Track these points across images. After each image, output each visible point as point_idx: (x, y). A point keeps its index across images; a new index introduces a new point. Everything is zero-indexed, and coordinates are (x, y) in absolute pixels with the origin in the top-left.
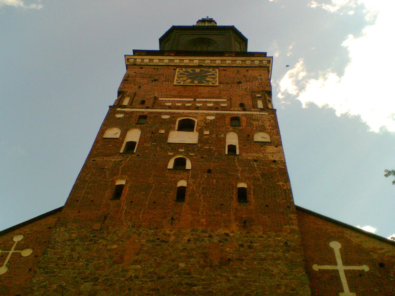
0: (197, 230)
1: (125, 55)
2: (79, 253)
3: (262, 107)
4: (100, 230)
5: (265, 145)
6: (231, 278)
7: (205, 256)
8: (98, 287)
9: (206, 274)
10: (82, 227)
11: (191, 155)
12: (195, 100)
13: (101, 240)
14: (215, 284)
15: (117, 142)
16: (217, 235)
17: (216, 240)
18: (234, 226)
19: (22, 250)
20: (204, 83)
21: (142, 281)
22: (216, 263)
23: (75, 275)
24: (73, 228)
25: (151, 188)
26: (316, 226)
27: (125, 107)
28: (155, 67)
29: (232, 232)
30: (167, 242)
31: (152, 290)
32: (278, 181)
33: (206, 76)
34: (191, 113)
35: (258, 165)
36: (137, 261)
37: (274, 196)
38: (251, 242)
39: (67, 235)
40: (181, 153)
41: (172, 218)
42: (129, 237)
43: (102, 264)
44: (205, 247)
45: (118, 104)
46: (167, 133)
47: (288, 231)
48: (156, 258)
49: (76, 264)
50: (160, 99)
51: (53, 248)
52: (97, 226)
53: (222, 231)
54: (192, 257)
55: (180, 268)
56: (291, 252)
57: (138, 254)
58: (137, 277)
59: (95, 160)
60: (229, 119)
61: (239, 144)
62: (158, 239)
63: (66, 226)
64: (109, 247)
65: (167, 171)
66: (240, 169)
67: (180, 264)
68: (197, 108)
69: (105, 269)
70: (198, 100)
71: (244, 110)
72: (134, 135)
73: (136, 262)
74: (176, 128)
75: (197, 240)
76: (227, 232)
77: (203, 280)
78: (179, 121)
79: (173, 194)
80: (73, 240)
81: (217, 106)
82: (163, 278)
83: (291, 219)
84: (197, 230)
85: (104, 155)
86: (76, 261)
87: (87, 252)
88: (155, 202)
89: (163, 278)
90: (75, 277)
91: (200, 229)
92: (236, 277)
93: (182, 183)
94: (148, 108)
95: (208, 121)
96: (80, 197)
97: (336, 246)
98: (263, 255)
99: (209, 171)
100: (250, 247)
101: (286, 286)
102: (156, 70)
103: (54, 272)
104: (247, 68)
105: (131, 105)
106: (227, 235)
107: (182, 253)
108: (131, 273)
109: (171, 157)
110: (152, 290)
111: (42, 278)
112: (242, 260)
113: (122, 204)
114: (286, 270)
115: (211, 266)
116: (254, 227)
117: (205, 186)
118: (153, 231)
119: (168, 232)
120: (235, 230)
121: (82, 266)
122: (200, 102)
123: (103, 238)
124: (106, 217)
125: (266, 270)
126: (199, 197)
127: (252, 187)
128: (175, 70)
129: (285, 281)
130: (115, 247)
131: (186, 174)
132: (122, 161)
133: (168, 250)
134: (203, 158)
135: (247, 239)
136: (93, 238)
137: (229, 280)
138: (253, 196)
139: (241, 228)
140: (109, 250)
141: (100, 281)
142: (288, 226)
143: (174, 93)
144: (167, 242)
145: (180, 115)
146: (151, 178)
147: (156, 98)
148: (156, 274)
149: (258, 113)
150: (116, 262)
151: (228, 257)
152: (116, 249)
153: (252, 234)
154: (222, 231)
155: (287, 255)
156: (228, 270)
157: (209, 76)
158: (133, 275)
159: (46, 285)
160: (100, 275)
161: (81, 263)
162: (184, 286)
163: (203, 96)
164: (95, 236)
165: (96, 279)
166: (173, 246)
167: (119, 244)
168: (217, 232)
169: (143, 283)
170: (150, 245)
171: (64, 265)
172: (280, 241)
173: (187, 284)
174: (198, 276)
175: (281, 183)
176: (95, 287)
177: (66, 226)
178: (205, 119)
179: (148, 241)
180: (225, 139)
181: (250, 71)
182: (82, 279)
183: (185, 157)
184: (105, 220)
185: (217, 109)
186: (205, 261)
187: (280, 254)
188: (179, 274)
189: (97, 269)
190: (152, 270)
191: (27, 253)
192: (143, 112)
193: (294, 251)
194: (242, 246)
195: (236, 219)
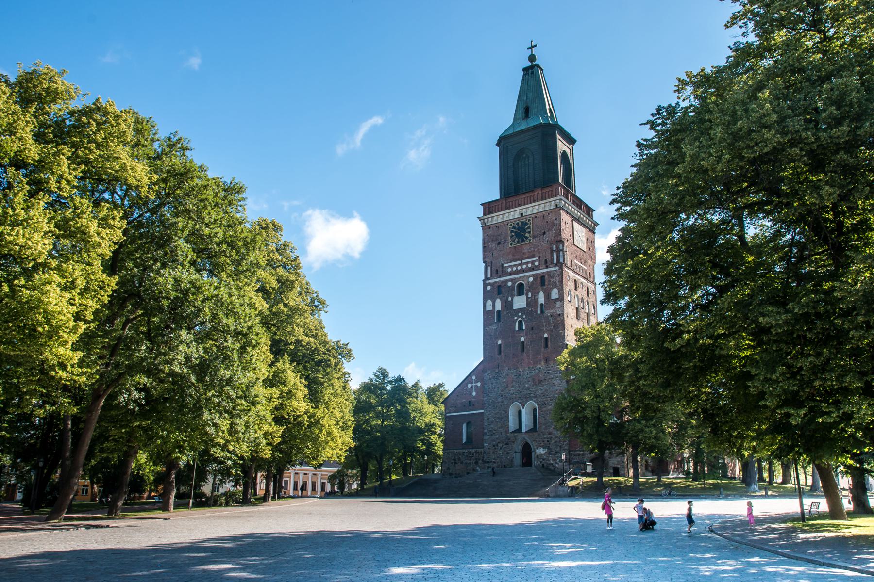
7: (533, 380)
18: (543, 363)
45: (486, 278)
53: (538, 366)
68: (523, 271)
71: (547, 267)
79: (520, 347)
93: (522, 339)
94: (500, 277)
120: (542, 365)
143: (511, 257)
147: (502, 265)
154: (538, 366)
185: (532, 269)
192: (498, 282)
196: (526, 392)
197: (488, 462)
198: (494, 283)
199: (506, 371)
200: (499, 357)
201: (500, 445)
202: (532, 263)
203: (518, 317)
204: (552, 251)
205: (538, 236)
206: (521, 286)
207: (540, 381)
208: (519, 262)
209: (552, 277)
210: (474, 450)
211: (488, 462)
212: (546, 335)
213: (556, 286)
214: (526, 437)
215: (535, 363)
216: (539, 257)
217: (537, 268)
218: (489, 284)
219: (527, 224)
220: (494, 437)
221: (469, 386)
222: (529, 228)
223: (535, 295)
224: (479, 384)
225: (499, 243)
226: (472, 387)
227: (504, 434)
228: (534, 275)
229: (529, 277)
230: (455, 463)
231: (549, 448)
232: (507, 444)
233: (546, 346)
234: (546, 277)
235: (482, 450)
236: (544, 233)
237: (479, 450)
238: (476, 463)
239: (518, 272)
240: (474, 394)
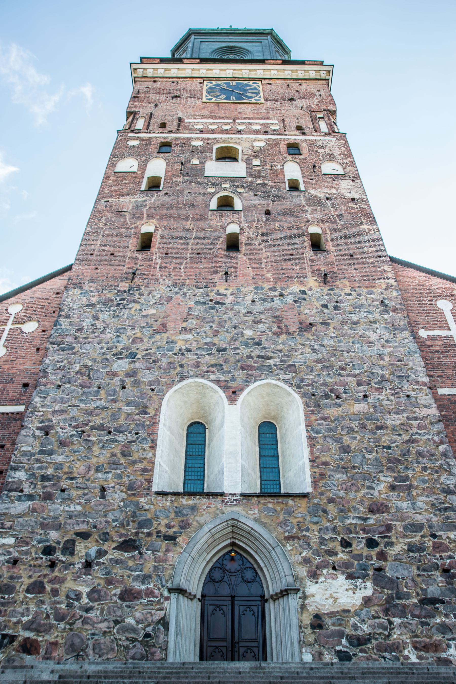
0: (263, 288)
1: (131, 64)
2: (104, 321)
3: (326, 130)
4: (129, 290)
5: (338, 178)
6: (316, 347)
7: (278, 320)
8: (137, 365)
9: (283, 343)
10: (103, 289)
11: (239, 191)
12: (234, 121)
13: (133, 304)
14: (297, 356)
15: (135, 177)
16: (290, 294)
17: (289, 299)
19: (23, 323)
20: (244, 99)
21: (197, 354)
22: (294, 328)
23: (102, 351)
24: (92, 289)
25: (191, 235)
26: (417, 282)
27: (139, 131)
28: (174, 80)
29: (311, 289)
30: (223, 304)
31: (212, 366)
32: (362, 224)
33: (246, 91)
34: (232, 139)
35: (332, 204)
36: (186, 329)
37: (360, 243)
38: (337, 302)
39: (85, 299)
40: (225, 189)
41: (226, 273)
42: (170, 299)
43: (139, 335)
44: (276, 309)
46: (203, 163)
47: (384, 287)
48: (211, 324)
49: (103, 336)
50: (186, 121)
51: (68, 317)
54: (260, 322)
55: (246, 337)
56: (391, 313)
57: (185, 320)
58: (189, 350)
59: (108, 201)
60: (285, 146)
61: (304, 177)
62: (211, 301)
63: (81, 288)
64: (144, 313)
65: (210, 212)
67: (245, 332)
69: (143, 341)
71: (304, 134)
72: (157, 167)
74: (214, 158)
75: (264, 300)
76: (303, 289)
77: (280, 351)
78: (217, 149)
80: (93, 305)
81: (265, 129)
82: (225, 350)
83: (385, 272)
84: (263, 288)
85: (119, 195)
86: (102, 332)
87: (115, 320)
88: (199, 254)
89: (225, 350)
90: (104, 354)
91: (267, 286)
92: (323, 346)
93: (233, 228)
95: (256, 149)
96: (94, 250)
97: (445, 306)
98: (355, 318)
99: (268, 213)
100: (336, 308)
101: (390, 355)
102: (175, 84)
103: (73, 348)
104: (300, 82)
105: (147, 129)
106: (304, 292)
107: (246, 318)
108: (181, 345)
109: (212, 195)
110: (212, 366)
111: (56, 358)
112: (328, 324)
113: (154, 257)
114: (387, 336)
115: (288, 333)
116: (338, 283)
117: (265, 231)
118: (201, 290)
119: (222, 291)
121: (111, 338)
123: (134, 301)
124: (134, 274)
125: (361, 336)
126: (259, 245)
127: (328, 231)
129: (387, 351)
130: (152, 311)
131: (236, 216)
132: (145, 201)
133: (226, 313)
134: (256, 195)
135: (331, 297)
136: (120, 302)
137: (314, 350)
138: (331, 243)
139: (322, 284)
140: (146, 316)
141: (139, 356)
142: (381, 281)
143: (205, 112)
144: (223, 304)
145: (217, 141)
146: (189, 223)
148: (215, 345)
149: (322, 138)
150: (156, 332)
151: (308, 321)
152: (154, 315)
153: (336, 291)
154: (296, 288)
155: (386, 317)
156: (311, 337)
157: (249, 91)
158: (184, 348)
159: (65, 366)
160: (138, 349)
161: (109, 335)
162: (255, 359)
163: (244, 116)
164: (124, 300)
165: (133, 355)
166: (232, 309)
167: (157, 309)
168: (289, 290)
169: (198, 358)
171: (86, 338)
173: (259, 357)
174: (273, 347)
175: (366, 227)
176: (132, 366)
177: (81, 288)
178: (253, 146)
179: (197, 303)
180: (282, 170)
181: (303, 85)
182: (114, 355)
183: (231, 195)
184: (133, 279)
185: (266, 132)
186: (279, 327)
187: (377, 316)
188: (247, 344)
189: (133, 342)
190: (208, 340)
191: (30, 327)
192: (165, 138)
193: (394, 311)
194: (325, 306)
195: (312, 273)
196: (244, 351)
199: (162, 289)
201: (85, 549)
214: (248, 516)
215: (283, 279)
220: (57, 508)
227: (116, 497)
228: (268, 140)
232: (128, 545)
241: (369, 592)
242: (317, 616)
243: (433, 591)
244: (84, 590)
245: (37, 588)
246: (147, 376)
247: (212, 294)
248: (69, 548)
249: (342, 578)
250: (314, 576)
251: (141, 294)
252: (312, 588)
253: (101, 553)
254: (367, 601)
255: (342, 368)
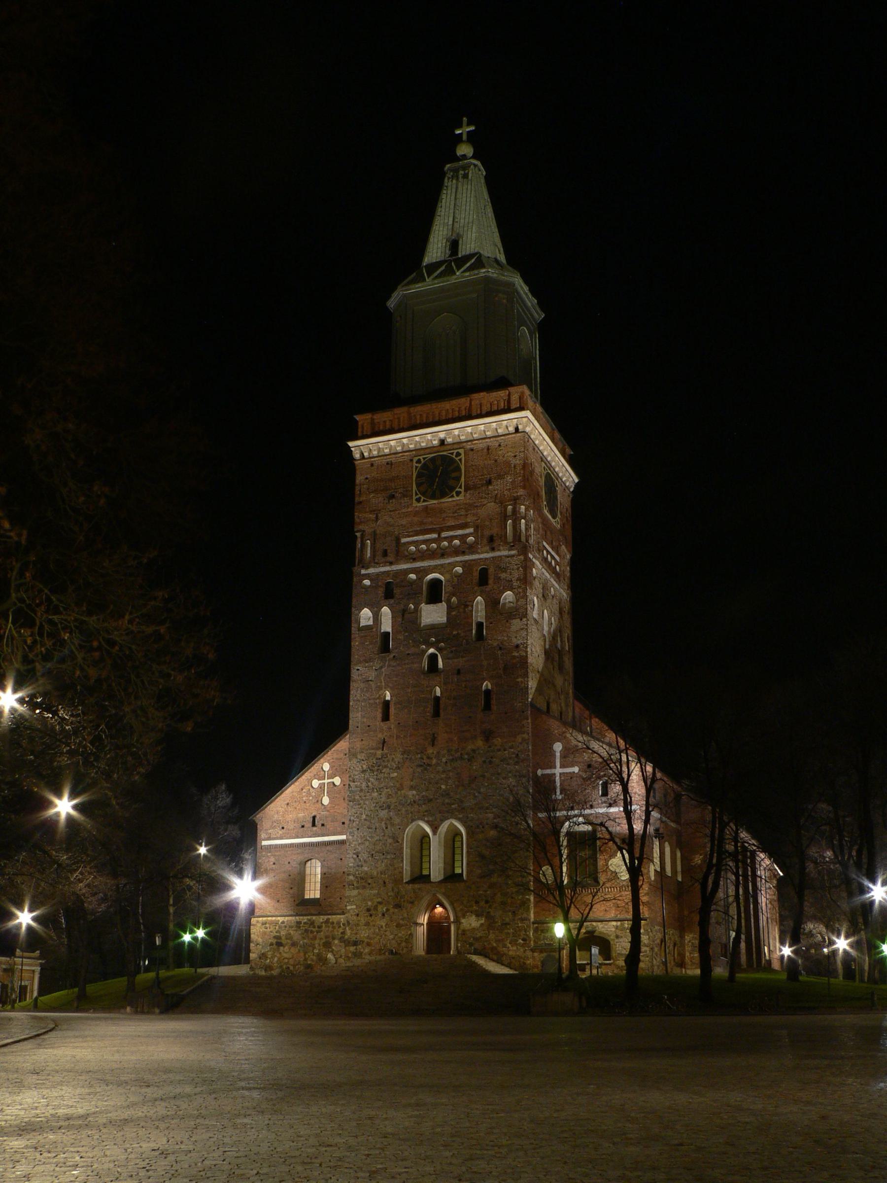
12: (439, 535)
18: (480, 743)
31: (426, 811)
52: (379, 752)
66: (485, 663)
70: (444, 535)
71: (493, 549)
73: (412, 788)
94: (391, 563)
100: (491, 762)
115: (463, 786)
122: (445, 539)
123: (386, 767)
128: (411, 460)
147: (398, 540)
154: (470, 747)
170: (419, 770)
172: (514, 753)
185: (463, 553)
188: (442, 795)
197: (355, 943)
198: (378, 574)
200: (384, 725)
202: (463, 538)
203: (431, 645)
204: (505, 517)
205: (475, 487)
206: (436, 585)
207: (473, 779)
208: (435, 536)
209: (504, 570)
210: (322, 918)
211: (355, 943)
212: (486, 685)
213: (511, 589)
216: (477, 528)
217: (472, 549)
218: (367, 576)
219: (452, 461)
221: (316, 783)
222: (458, 469)
223: (466, 605)
224: (337, 781)
225: (392, 497)
226: (322, 786)
228: (464, 564)
229: (454, 565)
230: (279, 944)
231: (489, 917)
233: (487, 707)
234: (491, 571)
235: (342, 918)
236: (489, 482)
237: (334, 918)
238: (327, 945)
239: (431, 555)
240: (326, 800)
241: (483, 921)
242: (464, 931)
243: (507, 920)
244: (384, 924)
245: (367, 924)
246: (397, 820)
247: (425, 757)
248: (376, 908)
249: (474, 917)
250: (464, 916)
251: (388, 761)
252: (463, 921)
253: (388, 910)
254: (482, 925)
255: (487, 808)
